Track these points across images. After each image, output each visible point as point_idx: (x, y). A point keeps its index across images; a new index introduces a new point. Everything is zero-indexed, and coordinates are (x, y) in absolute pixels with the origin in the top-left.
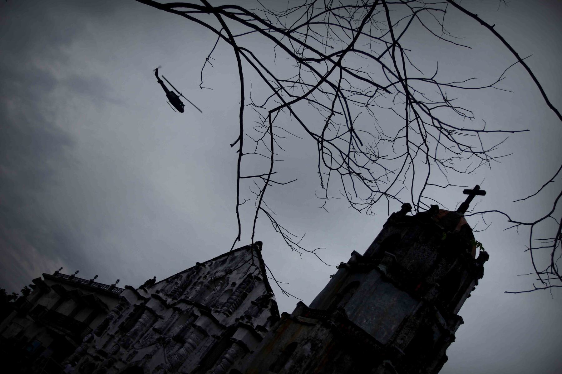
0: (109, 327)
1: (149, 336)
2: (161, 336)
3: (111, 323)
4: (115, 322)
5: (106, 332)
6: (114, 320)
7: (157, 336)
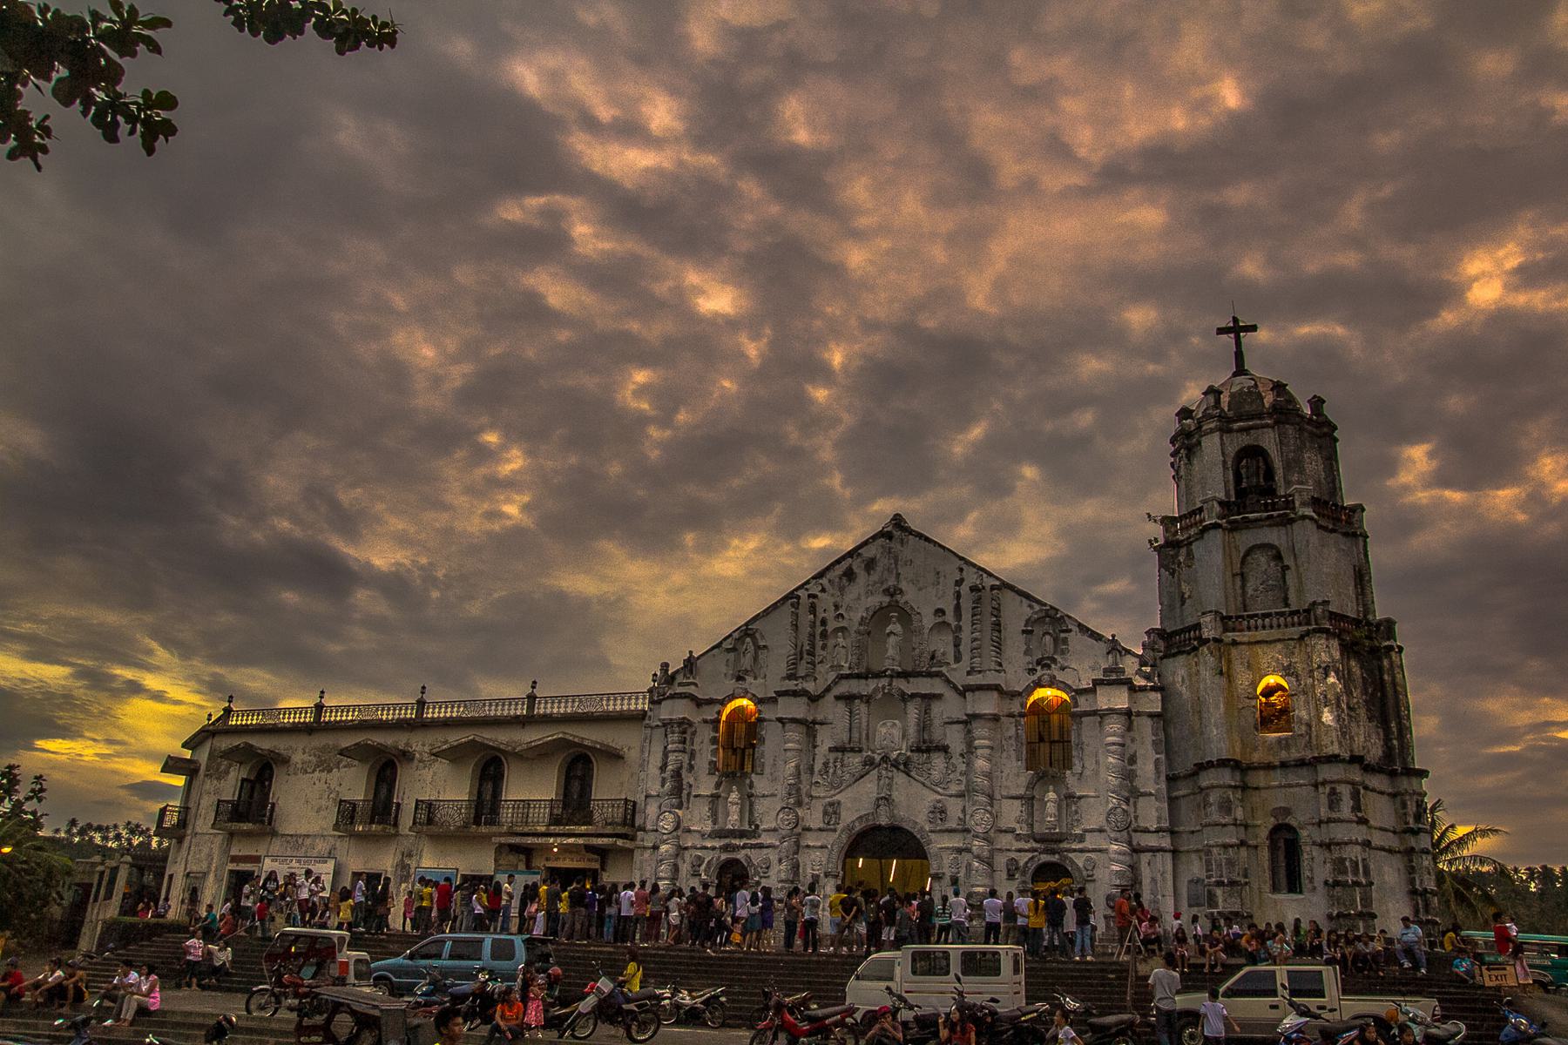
0: (684, 783)
1: (831, 765)
2: (865, 754)
3: (684, 773)
4: (691, 767)
5: (689, 794)
6: (685, 765)
7: (855, 761)
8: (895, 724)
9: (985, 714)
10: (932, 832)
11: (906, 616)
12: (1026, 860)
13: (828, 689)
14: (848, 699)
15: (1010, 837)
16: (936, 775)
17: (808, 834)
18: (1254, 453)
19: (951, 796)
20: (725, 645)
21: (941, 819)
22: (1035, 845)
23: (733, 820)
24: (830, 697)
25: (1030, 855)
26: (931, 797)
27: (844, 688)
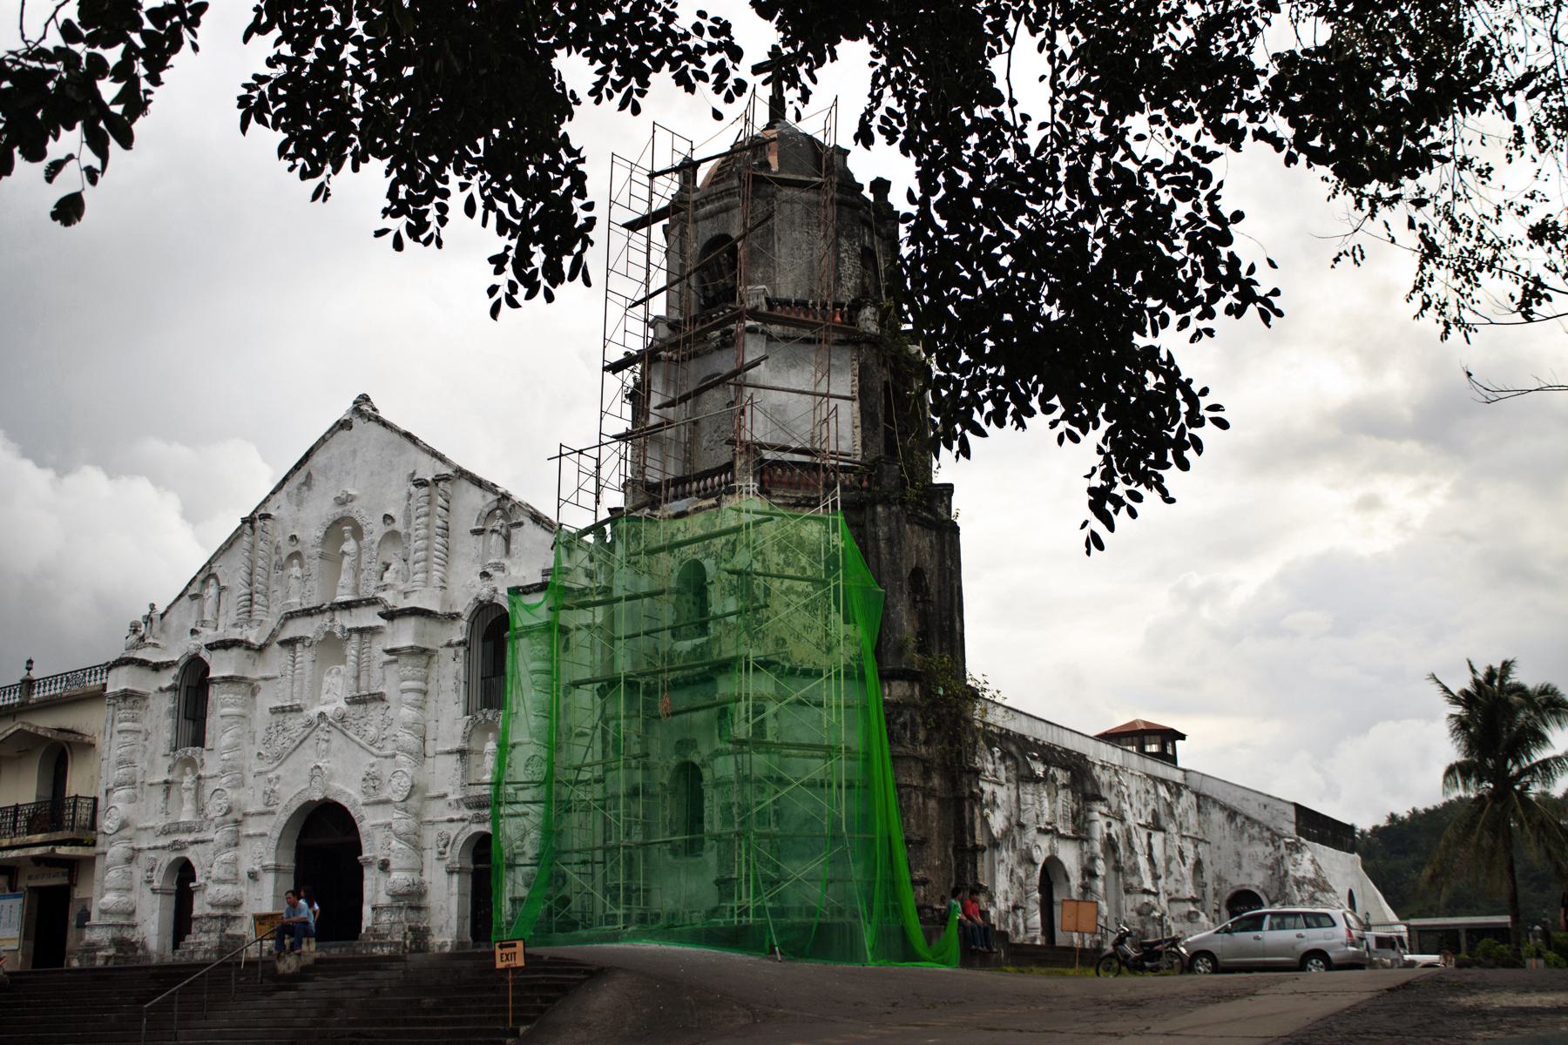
9: (403, 648)
10: (365, 804)
13: (273, 635)
14: (290, 643)
15: (441, 803)
16: (372, 731)
17: (250, 820)
19: (386, 757)
20: (192, 591)
22: (470, 813)
23: (186, 815)
25: (461, 825)
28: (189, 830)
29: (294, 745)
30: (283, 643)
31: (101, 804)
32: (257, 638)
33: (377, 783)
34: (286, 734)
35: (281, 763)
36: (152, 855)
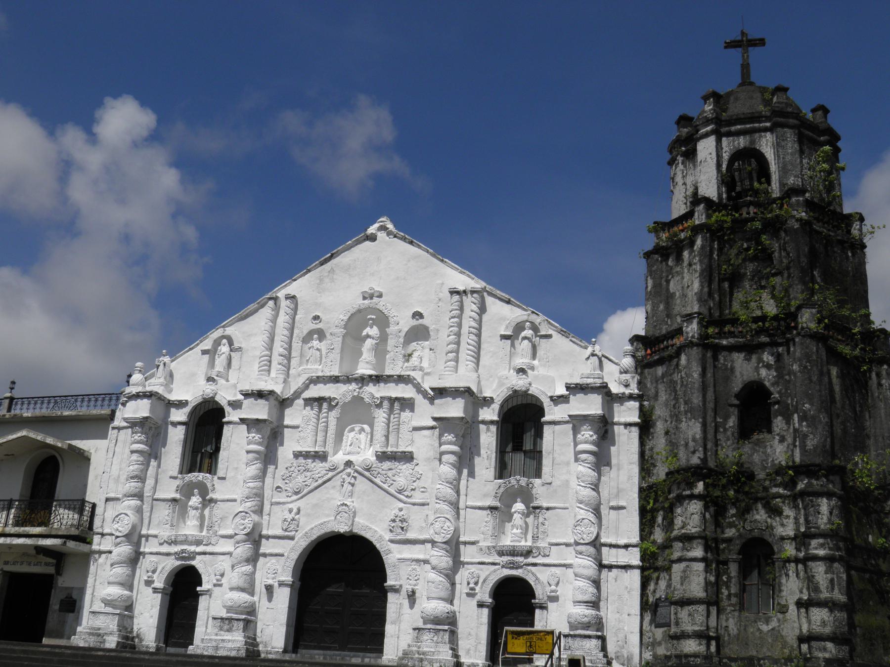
8: (363, 430)
10: (392, 541)
11: (383, 321)
12: (487, 573)
13: (297, 395)
18: (752, 155)
19: (414, 504)
21: (402, 528)
23: (190, 528)
24: (300, 402)
26: (393, 508)
27: (315, 391)
28: (198, 543)
29: (316, 484)
30: (309, 402)
31: (99, 511)
32: (282, 393)
33: (405, 524)
34: (308, 474)
35: (302, 497)
36: (154, 558)
